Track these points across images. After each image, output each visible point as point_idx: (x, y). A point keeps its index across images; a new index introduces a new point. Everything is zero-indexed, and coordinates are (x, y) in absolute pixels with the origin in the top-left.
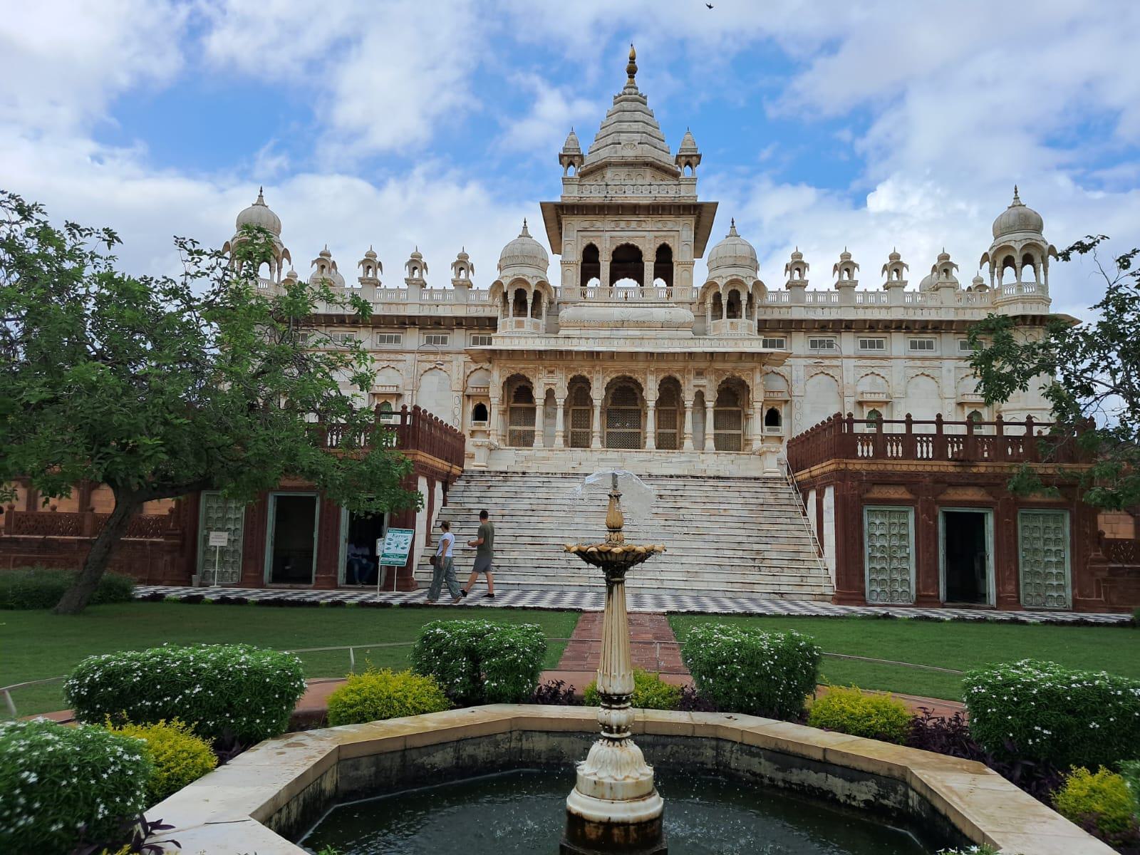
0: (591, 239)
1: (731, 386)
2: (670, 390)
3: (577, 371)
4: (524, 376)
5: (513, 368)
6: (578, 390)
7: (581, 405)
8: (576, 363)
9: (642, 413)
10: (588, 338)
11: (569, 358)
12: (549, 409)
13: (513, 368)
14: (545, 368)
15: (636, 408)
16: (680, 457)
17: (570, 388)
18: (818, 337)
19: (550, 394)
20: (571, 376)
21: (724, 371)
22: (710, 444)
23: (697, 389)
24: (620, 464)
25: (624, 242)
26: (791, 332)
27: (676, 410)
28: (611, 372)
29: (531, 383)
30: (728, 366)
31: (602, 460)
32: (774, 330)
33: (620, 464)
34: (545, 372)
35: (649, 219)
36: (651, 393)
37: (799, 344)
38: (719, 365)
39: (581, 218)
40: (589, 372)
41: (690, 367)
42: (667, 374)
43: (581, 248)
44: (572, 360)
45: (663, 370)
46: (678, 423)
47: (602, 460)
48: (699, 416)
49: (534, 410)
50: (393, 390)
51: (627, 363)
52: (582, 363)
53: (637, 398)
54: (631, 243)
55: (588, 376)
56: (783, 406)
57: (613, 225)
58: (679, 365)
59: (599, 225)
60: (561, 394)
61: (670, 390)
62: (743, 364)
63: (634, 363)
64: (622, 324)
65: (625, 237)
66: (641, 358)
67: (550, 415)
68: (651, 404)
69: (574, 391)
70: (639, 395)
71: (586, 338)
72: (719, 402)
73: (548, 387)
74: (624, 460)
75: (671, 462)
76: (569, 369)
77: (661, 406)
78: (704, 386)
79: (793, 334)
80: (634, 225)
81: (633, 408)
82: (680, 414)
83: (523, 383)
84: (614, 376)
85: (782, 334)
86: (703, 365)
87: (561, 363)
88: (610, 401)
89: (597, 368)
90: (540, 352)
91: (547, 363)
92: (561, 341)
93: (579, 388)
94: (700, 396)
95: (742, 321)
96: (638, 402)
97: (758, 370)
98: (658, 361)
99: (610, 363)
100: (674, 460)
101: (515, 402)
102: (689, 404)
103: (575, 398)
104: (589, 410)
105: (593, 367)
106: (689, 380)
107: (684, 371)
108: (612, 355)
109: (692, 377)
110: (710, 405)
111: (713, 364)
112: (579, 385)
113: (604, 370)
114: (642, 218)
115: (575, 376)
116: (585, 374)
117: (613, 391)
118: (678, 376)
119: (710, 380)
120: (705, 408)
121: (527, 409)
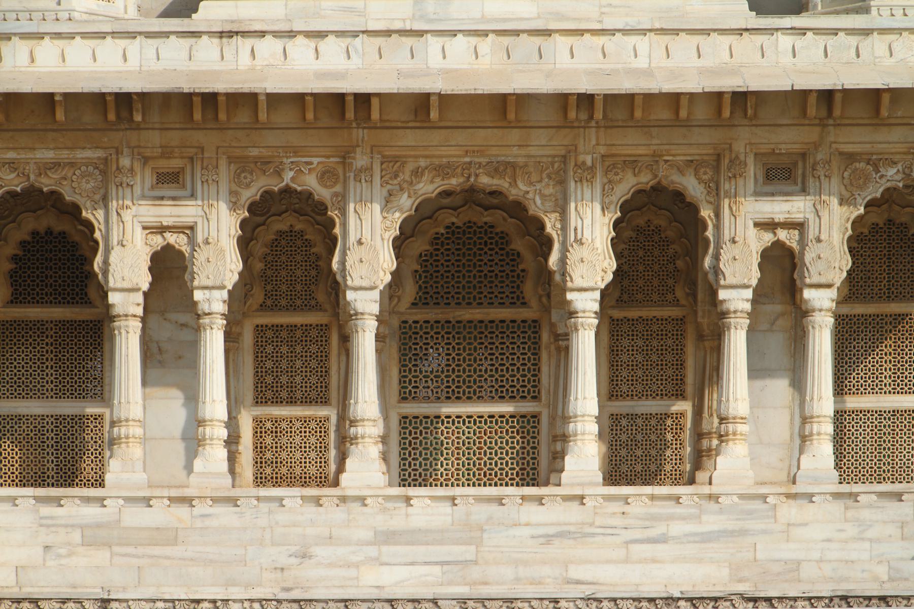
1: (903, 216)
2: (663, 250)
3: (279, 173)
4: (55, 197)
5: (12, 165)
6: (274, 244)
7: (292, 308)
8: (272, 139)
9: (545, 336)
10: (321, 35)
11: (243, 117)
12: (163, 331)
13: (12, 165)
14: (146, 160)
15: (505, 313)
16: (698, 518)
17: (244, 244)
19: (170, 270)
20: (250, 194)
22: (822, 453)
23: (768, 238)
24: (468, 552)
27: (682, 319)
28: (417, 173)
29: (90, 226)
30: (892, 139)
31: (389, 537)
33: (468, 552)
34: (143, 179)
38: (856, 139)
40: (327, 176)
41: (739, 147)
42: (645, 179)
45: (632, 164)
46: (690, 379)
47: (389, 537)
48: (776, 342)
49: (96, 333)
51: (481, 136)
52: (295, 138)
53: (521, 276)
55: (322, 193)
58: (702, 140)
60: (219, 268)
61: (663, 250)
63: (514, 136)
67: (168, 358)
68: (586, 303)
69: (259, 249)
70: (529, 262)
71: (309, 34)
72: (855, 287)
73: (158, 242)
74: (473, 534)
75: (662, 540)
76: (244, 167)
77: (620, 303)
81: (505, 313)
82: (700, 337)
83: (47, 221)
86: (788, 139)
87: (209, 139)
88: (410, 291)
89: (360, 160)
90: (125, 100)
91: (154, 139)
92: (208, 49)
93: (290, 255)
94: (782, 270)
96: (528, 288)
98: (609, 124)
99: (409, 138)
100: (677, 529)
101: (15, 300)
102: (737, 299)
103: (265, 278)
104: (324, 329)
105: (345, 157)
107: (719, 168)
108: (420, 107)
110: (822, 301)
112: (280, 225)
113: (393, 164)
115: (267, 195)
116: (311, 183)
117: (420, 245)
118: (693, 187)
120: (800, 314)
121: (64, 325)
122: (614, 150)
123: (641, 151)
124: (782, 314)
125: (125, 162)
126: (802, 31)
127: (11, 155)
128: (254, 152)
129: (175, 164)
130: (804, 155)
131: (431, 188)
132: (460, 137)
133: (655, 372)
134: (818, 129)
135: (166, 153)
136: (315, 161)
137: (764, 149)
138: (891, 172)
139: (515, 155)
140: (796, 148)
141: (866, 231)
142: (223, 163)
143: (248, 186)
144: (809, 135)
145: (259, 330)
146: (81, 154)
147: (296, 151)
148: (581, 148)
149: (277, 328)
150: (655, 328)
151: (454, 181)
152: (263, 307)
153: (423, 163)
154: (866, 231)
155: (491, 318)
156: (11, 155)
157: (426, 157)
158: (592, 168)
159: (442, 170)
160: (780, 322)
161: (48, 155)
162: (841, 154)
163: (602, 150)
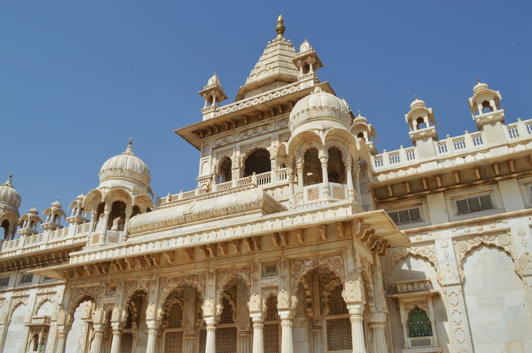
0: (225, 153)
3: (136, 285)
5: (82, 289)
8: (135, 274)
14: (107, 285)
18: (466, 195)
21: (303, 260)
25: (253, 148)
26: (424, 196)
30: (306, 252)
32: (402, 198)
35: (273, 121)
36: (210, 309)
37: (438, 208)
39: (215, 136)
41: (256, 261)
43: (216, 162)
44: (131, 272)
50: (41, 322)
52: (140, 274)
54: (259, 146)
55: (147, 289)
56: (430, 304)
57: (242, 135)
59: (231, 139)
62: (327, 246)
64: (185, 220)
65: (253, 142)
66: (200, 255)
76: (128, 284)
78: (276, 288)
79: (429, 197)
80: (260, 130)
84: (173, 286)
85: (414, 202)
95: (324, 185)
97: (349, 252)
104: (182, 332)
106: (256, 280)
107: (249, 269)
109: (258, 275)
111: (286, 252)
114: (266, 121)
118: (244, 276)
119: (283, 277)
122: (220, 267)
123: (227, 266)
124: (305, 321)
125: (103, 285)
126: (275, 219)
127: (82, 286)
128: (130, 279)
129: (113, 285)
130: (277, 261)
131: (172, 285)
132: (179, 268)
133: (270, 344)
134: (281, 251)
135: (112, 281)
136: (146, 280)
137: (264, 261)
138: (308, 263)
139: (193, 272)
140: (274, 259)
141: (334, 289)
142: (123, 284)
143: (129, 290)
144: (279, 253)
145: (167, 334)
146: (95, 284)
147: (139, 277)
148: (210, 267)
149: (171, 333)
150: (269, 328)
151: (178, 282)
152: (169, 327)
153: (171, 277)
154: (334, 289)
155: (224, 327)
156: (82, 286)
157: (172, 276)
158: (213, 273)
159: (176, 279)
160: (304, 324)
161: (88, 285)
162: (290, 259)
163: (216, 267)
